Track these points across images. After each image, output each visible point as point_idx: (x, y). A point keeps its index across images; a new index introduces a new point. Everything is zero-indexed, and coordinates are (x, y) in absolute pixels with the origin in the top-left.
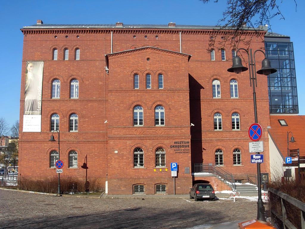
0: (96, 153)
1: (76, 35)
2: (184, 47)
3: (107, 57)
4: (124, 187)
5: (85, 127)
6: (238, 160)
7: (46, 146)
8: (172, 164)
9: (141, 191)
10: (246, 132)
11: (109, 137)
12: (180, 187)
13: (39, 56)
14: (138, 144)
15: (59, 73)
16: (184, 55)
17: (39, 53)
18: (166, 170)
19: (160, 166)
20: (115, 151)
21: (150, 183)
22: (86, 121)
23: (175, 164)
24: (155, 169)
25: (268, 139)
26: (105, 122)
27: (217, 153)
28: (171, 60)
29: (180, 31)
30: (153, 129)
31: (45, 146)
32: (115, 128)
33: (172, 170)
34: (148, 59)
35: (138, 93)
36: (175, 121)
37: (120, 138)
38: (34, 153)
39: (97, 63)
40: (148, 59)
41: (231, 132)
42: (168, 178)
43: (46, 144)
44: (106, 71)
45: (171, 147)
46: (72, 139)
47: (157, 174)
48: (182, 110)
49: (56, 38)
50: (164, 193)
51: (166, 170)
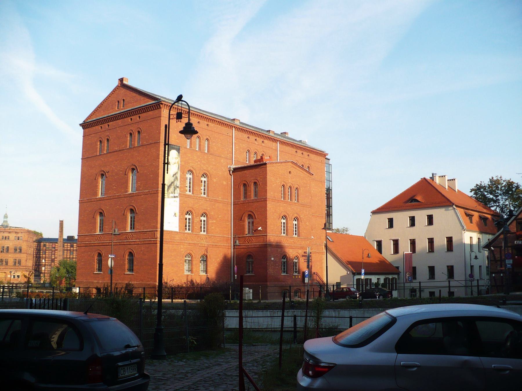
31: (181, 248)
38: (172, 255)
43: (182, 246)
45: (303, 256)
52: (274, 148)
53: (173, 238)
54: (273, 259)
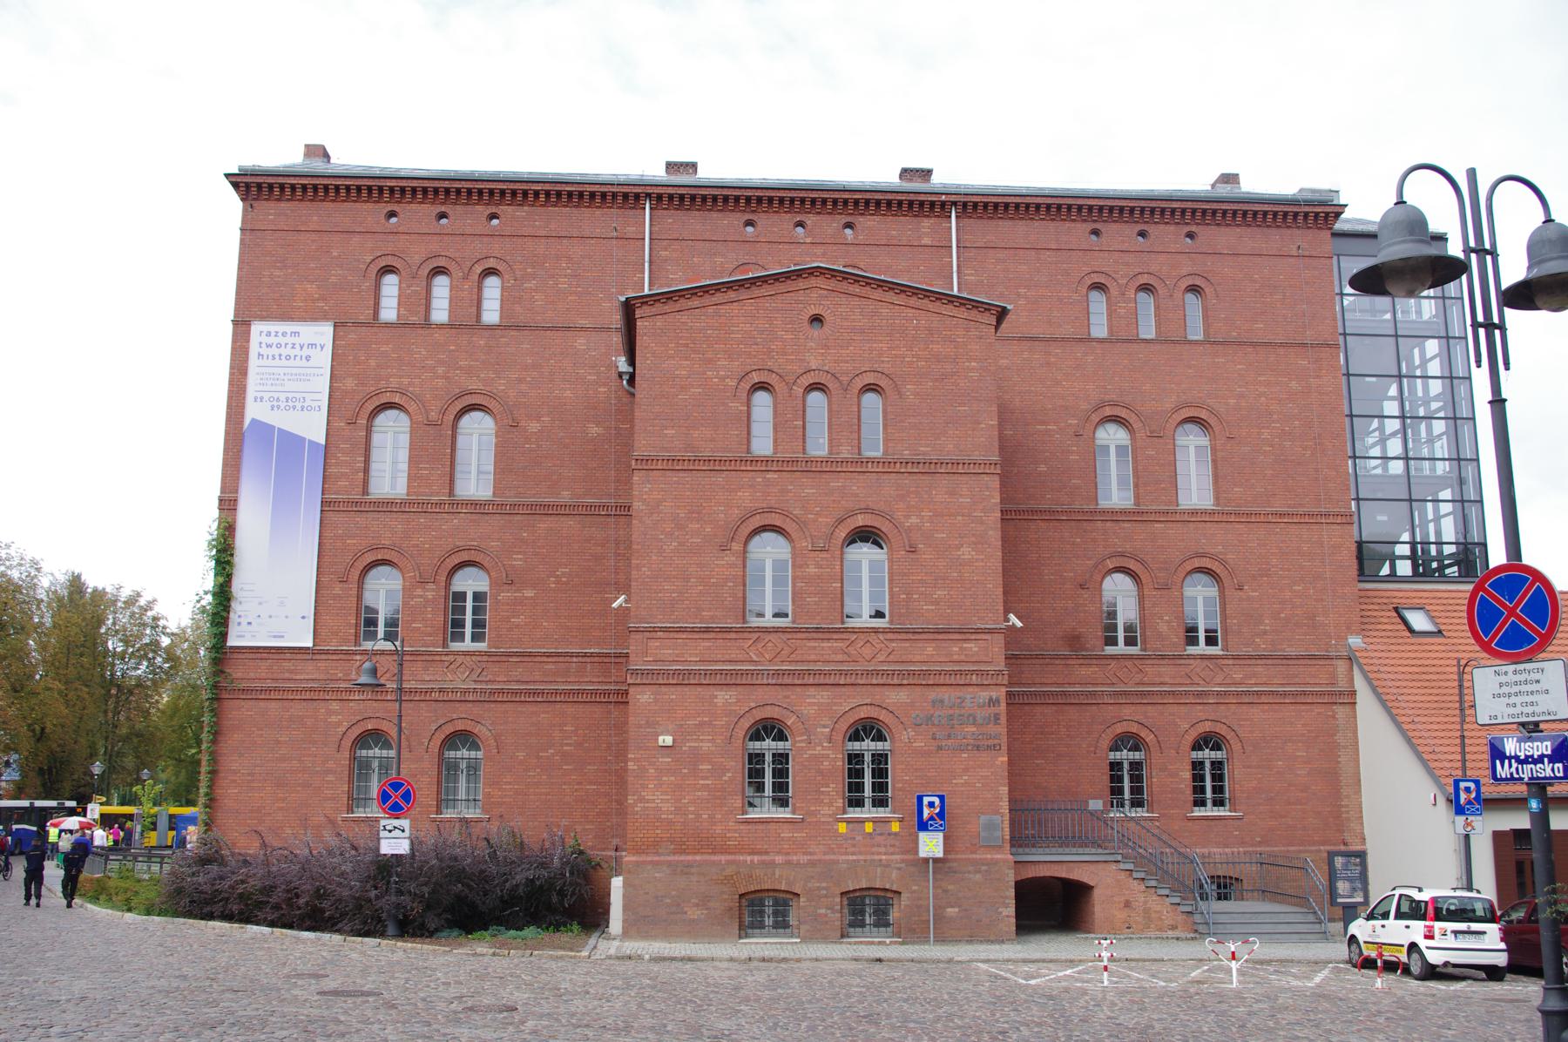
0: (567, 745)
1: (483, 210)
2: (972, 275)
3: (629, 308)
4: (697, 905)
5: (517, 626)
6: (1215, 790)
7: (336, 713)
8: (920, 799)
9: (776, 926)
10: (1248, 662)
11: (635, 672)
12: (957, 910)
13: (314, 301)
14: (769, 708)
15: (406, 381)
16: (976, 305)
17: (311, 288)
18: (895, 827)
19: (867, 812)
20: (662, 734)
21: (819, 888)
22: (527, 598)
23: (937, 801)
24: (842, 820)
25: (1353, 693)
26: (615, 605)
27: (1118, 753)
28: (916, 328)
29: (955, 203)
30: (835, 636)
32: (663, 630)
33: (923, 826)
34: (817, 319)
35: (769, 475)
36: (936, 603)
37: (683, 679)
38: (278, 742)
39: (581, 342)
40: (817, 319)
41: (1181, 657)
42: (903, 865)
43: (335, 706)
44: (620, 375)
46: (459, 680)
47: (854, 846)
48: (966, 553)
49: (394, 220)
50: (881, 936)
51: (895, 827)
52: (926, 241)
53: (287, 675)
54: (667, 740)
